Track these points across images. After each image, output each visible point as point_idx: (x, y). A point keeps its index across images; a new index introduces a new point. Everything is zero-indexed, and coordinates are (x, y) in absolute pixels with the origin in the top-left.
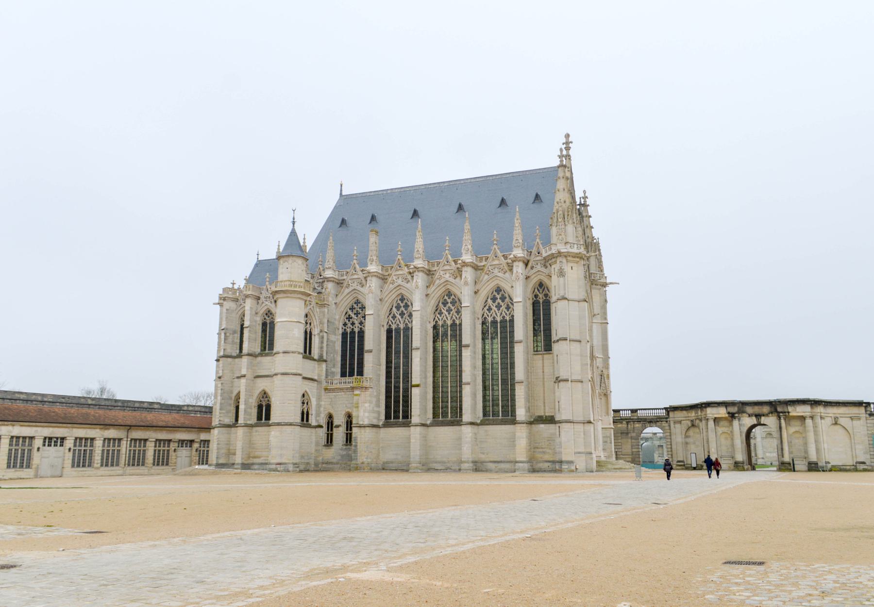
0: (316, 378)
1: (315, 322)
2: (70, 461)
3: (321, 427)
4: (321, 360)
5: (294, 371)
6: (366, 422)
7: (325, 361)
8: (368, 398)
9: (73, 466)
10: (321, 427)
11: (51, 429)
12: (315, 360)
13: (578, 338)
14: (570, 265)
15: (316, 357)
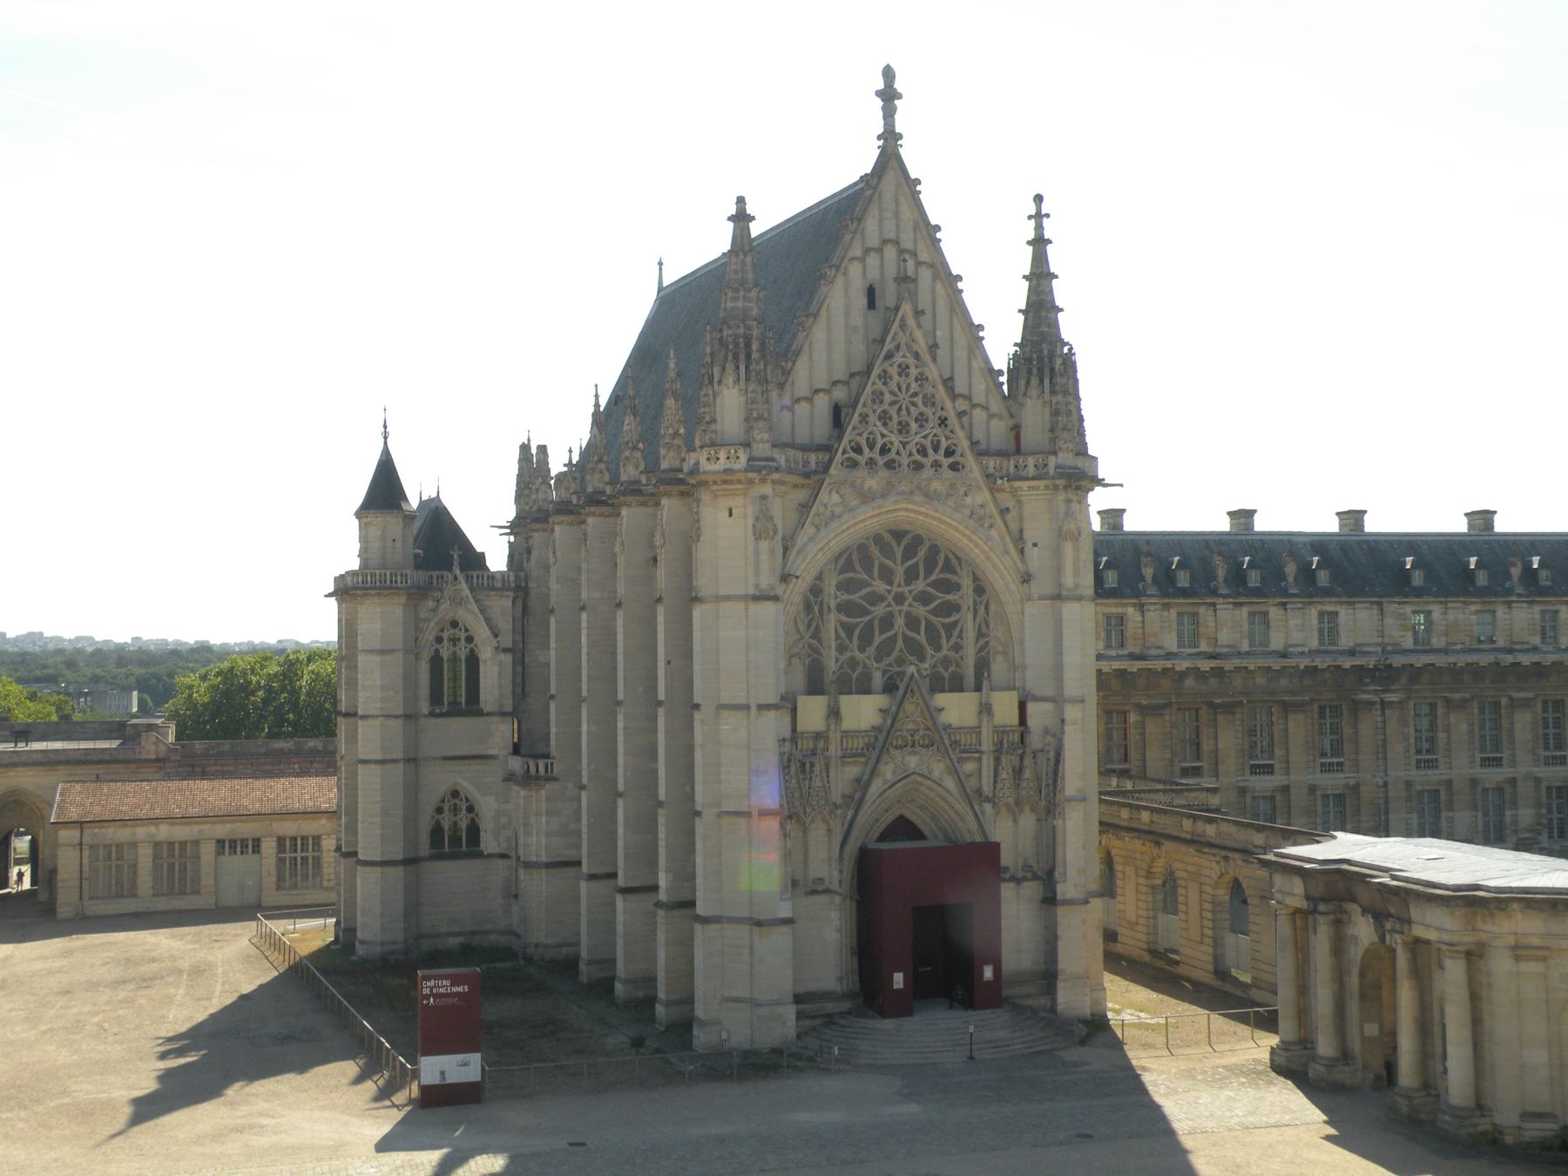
0: (494, 752)
1: (481, 632)
2: (274, 879)
3: (503, 856)
4: (503, 714)
5: (378, 757)
6: (544, 859)
7: (514, 713)
8: (544, 806)
9: (278, 888)
10: (503, 856)
11: (229, 826)
12: (489, 714)
13: (744, 702)
14: (724, 503)
15: (488, 709)
